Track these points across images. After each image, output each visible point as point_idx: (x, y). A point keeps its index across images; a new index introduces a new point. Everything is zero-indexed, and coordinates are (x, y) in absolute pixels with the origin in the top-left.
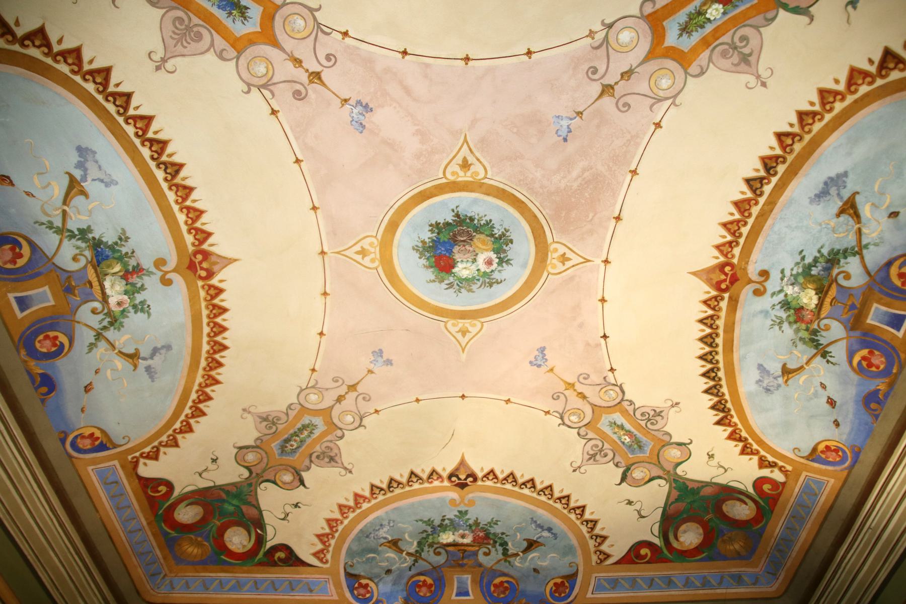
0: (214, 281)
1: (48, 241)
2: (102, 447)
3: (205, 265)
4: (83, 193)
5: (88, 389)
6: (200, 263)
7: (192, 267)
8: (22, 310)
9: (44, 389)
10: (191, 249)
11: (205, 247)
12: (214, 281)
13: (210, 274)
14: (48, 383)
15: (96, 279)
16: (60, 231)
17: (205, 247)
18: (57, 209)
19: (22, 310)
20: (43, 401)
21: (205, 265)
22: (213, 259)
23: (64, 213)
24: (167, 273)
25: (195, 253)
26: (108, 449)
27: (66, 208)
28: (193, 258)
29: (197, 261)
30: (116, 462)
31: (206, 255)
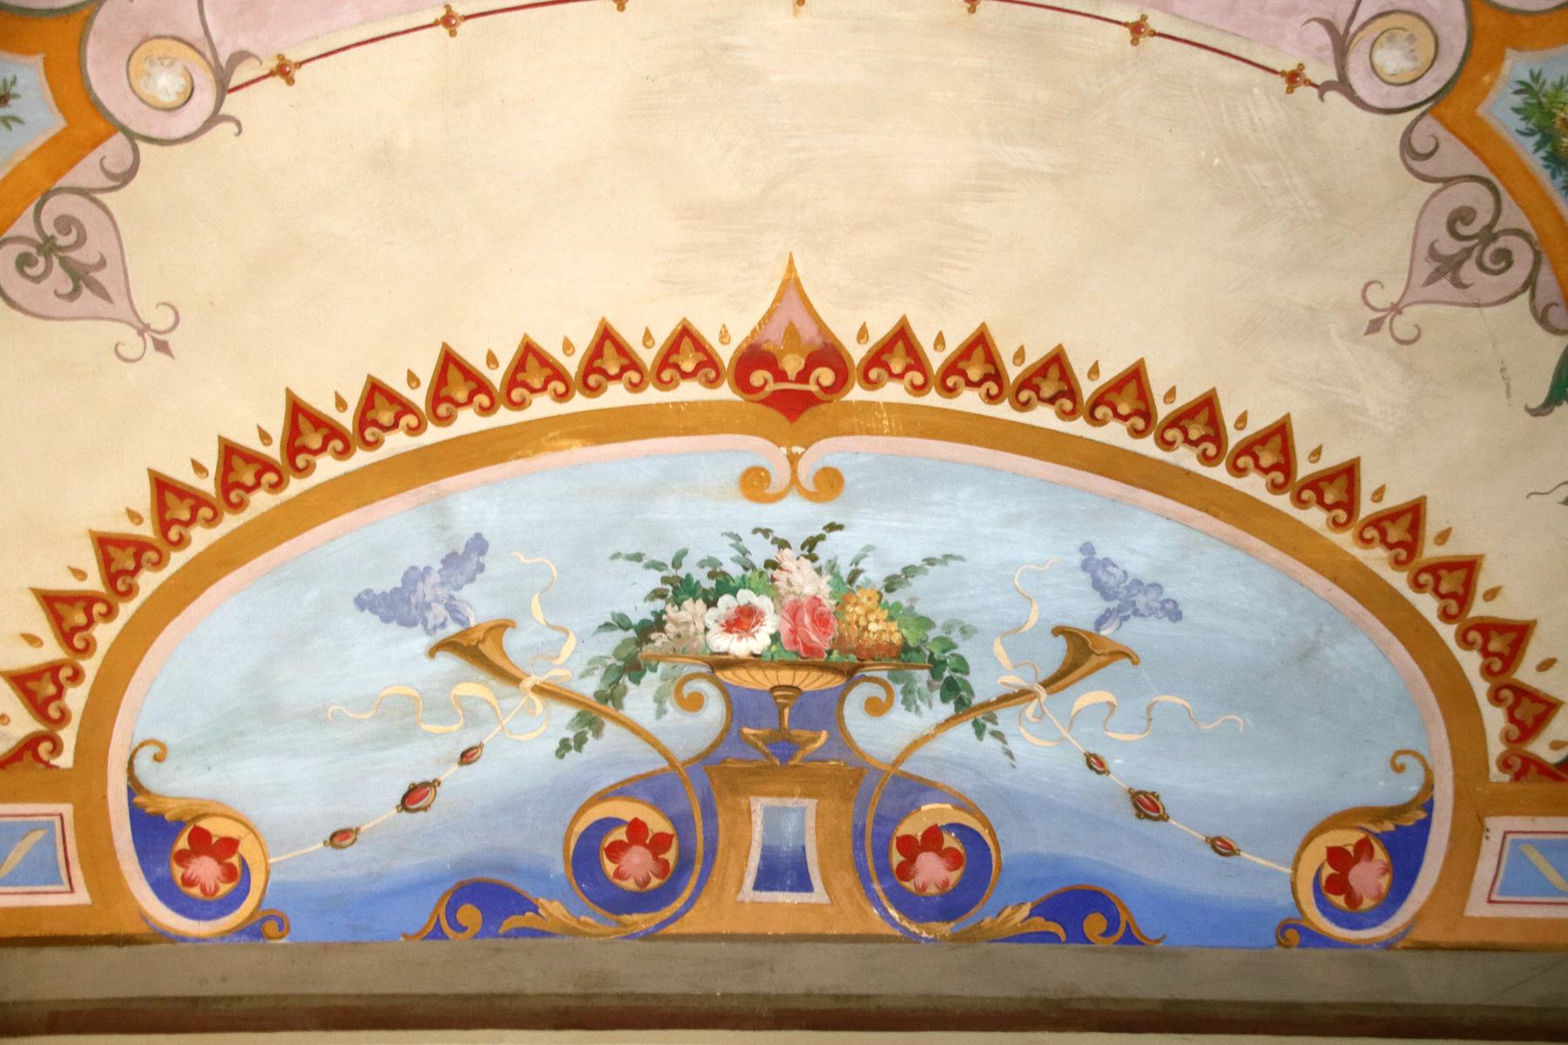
0: (857, 353)
1: (613, 753)
2: (1403, 841)
3: (792, 364)
4: (499, 628)
5: (1146, 805)
6: (780, 376)
7: (793, 405)
8: (804, 884)
9: (1095, 924)
10: (725, 392)
11: (726, 355)
12: (857, 353)
13: (828, 354)
14: (1076, 907)
15: (771, 674)
16: (590, 719)
17: (726, 355)
18: (530, 706)
19: (804, 884)
20: (1130, 938)
21: (792, 364)
22: (774, 339)
23: (539, 690)
24: (794, 479)
25: (742, 383)
26: (1425, 825)
27: (528, 683)
28: (761, 395)
29: (772, 387)
30: (1497, 825)
31: (754, 358)
